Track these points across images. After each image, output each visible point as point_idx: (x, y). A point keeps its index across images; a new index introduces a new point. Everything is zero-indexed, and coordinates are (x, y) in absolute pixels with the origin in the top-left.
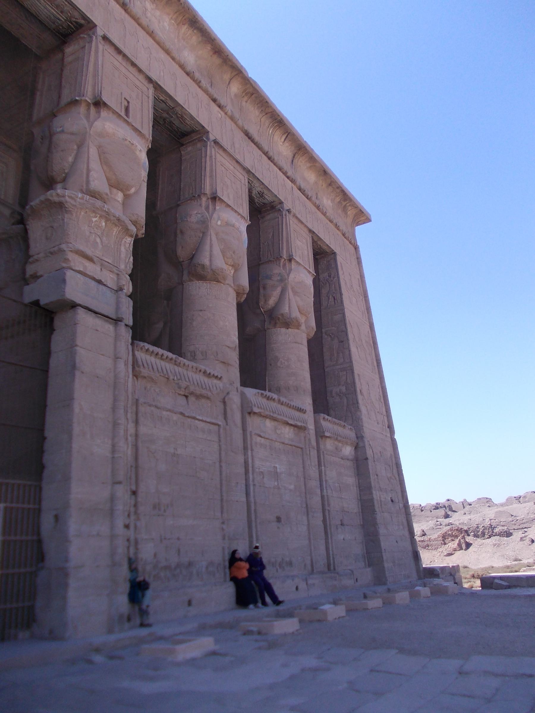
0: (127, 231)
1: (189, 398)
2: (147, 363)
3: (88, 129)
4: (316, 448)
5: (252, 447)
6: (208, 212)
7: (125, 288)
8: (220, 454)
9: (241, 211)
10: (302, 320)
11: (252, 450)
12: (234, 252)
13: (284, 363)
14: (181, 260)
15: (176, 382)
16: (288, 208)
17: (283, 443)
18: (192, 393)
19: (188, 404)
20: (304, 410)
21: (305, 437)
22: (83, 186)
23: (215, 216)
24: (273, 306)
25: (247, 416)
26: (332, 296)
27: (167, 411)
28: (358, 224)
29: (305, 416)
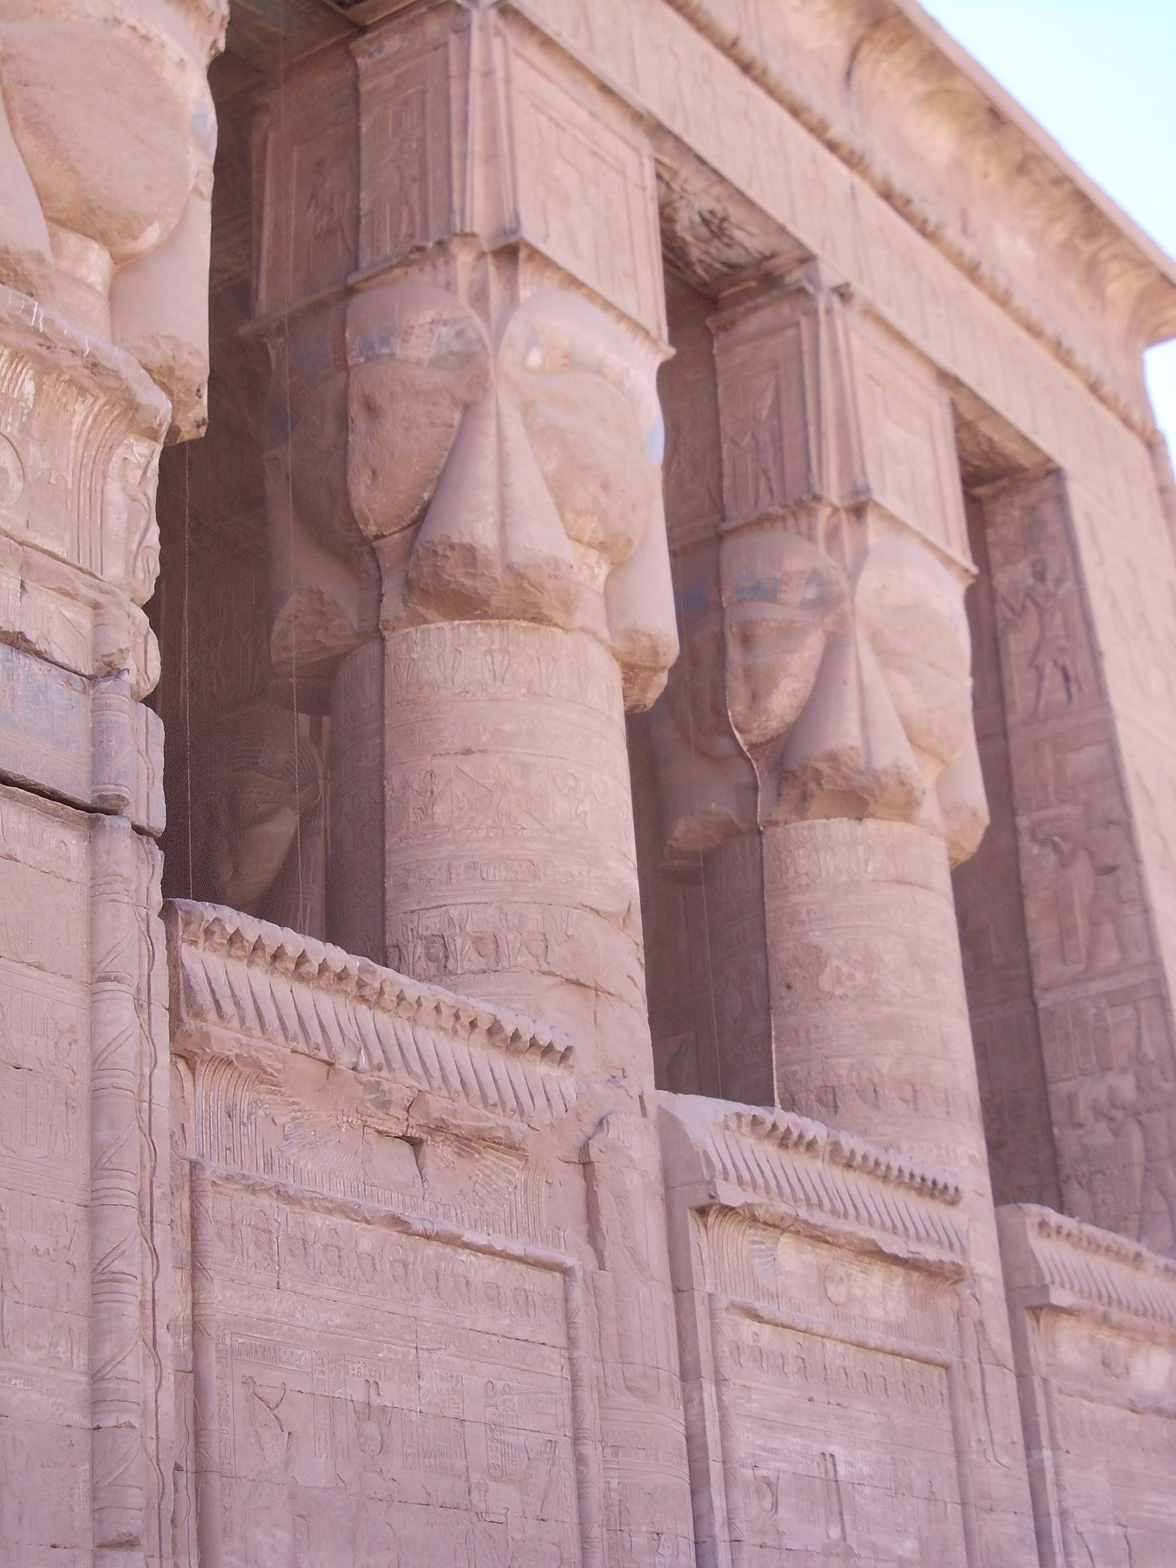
0: (128, 408)
1: (427, 1149)
2: (234, 995)
4: (1011, 1363)
5: (717, 1370)
6: (485, 314)
7: (130, 664)
8: (575, 1401)
9: (629, 305)
10: (924, 776)
11: (720, 1381)
12: (606, 487)
13: (851, 977)
14: (372, 530)
15: (364, 1078)
16: (837, 281)
17: (860, 1345)
18: (439, 1127)
19: (423, 1179)
20: (951, 1191)
21: (959, 1315)
23: (516, 328)
24: (790, 717)
25: (692, 1221)
26: (1055, 662)
27: (330, 1211)
29: (957, 1217)
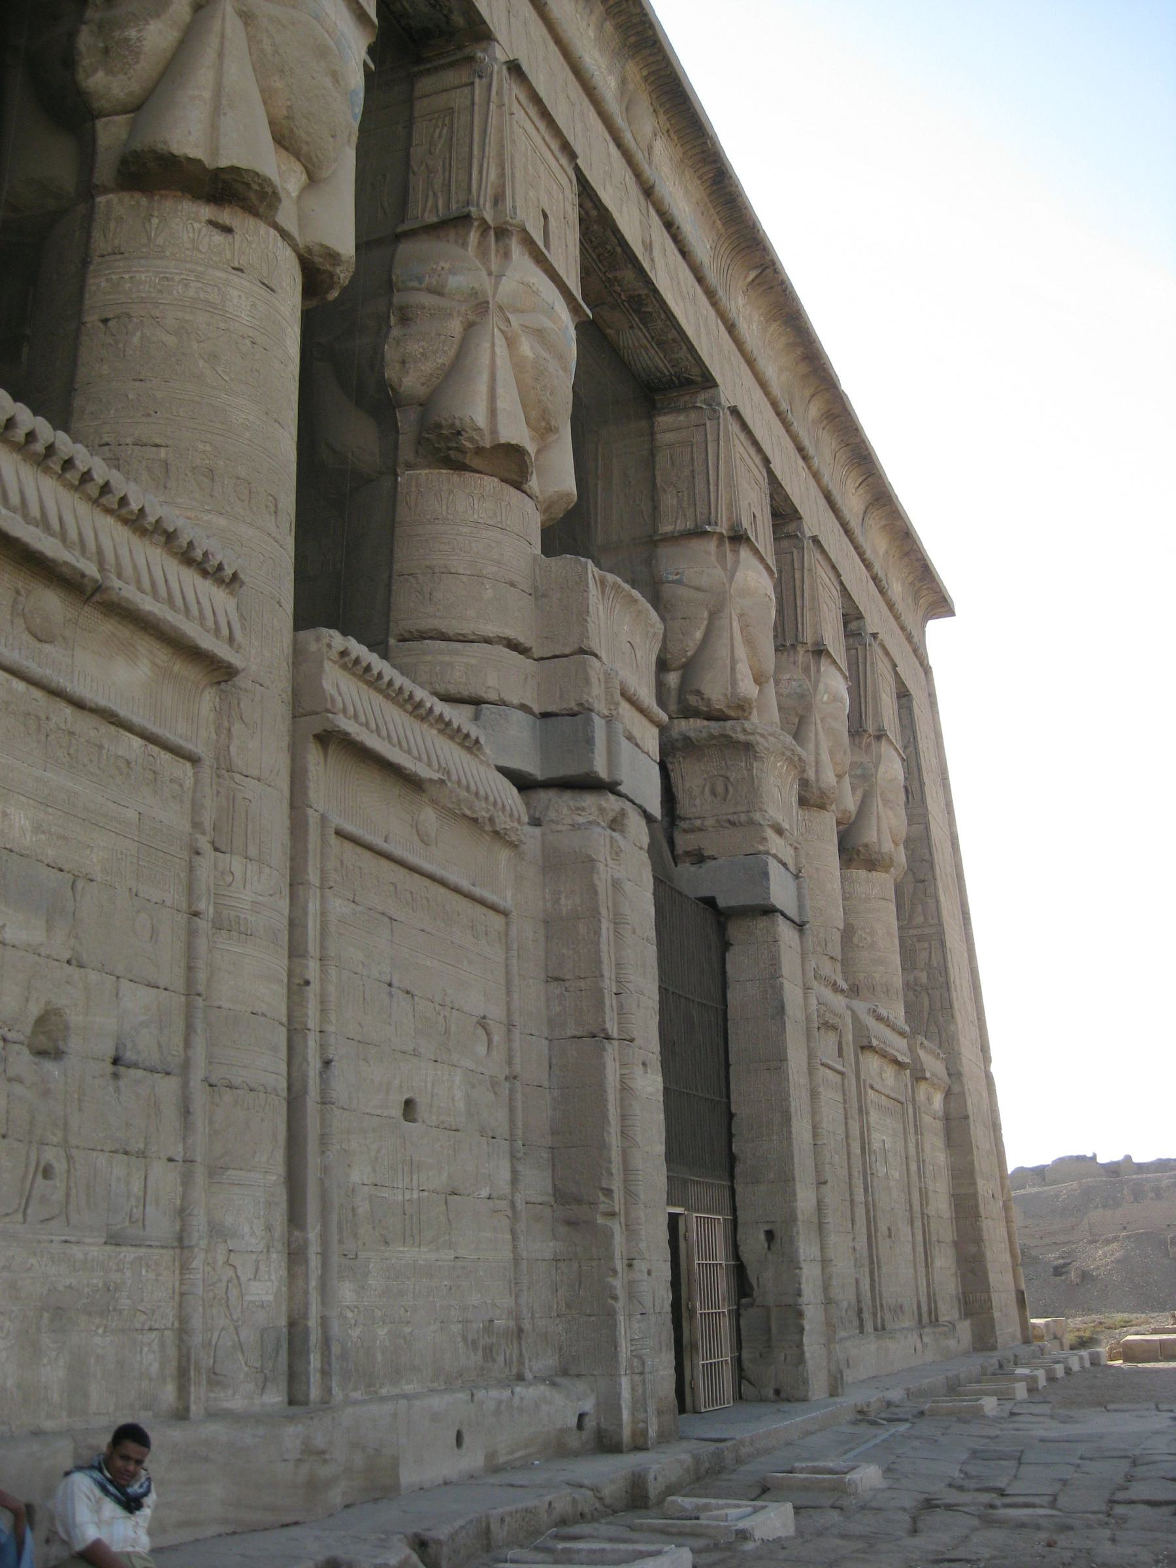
3: (727, 585)
6: (809, 677)
22: (727, 689)
28: (931, 618)
